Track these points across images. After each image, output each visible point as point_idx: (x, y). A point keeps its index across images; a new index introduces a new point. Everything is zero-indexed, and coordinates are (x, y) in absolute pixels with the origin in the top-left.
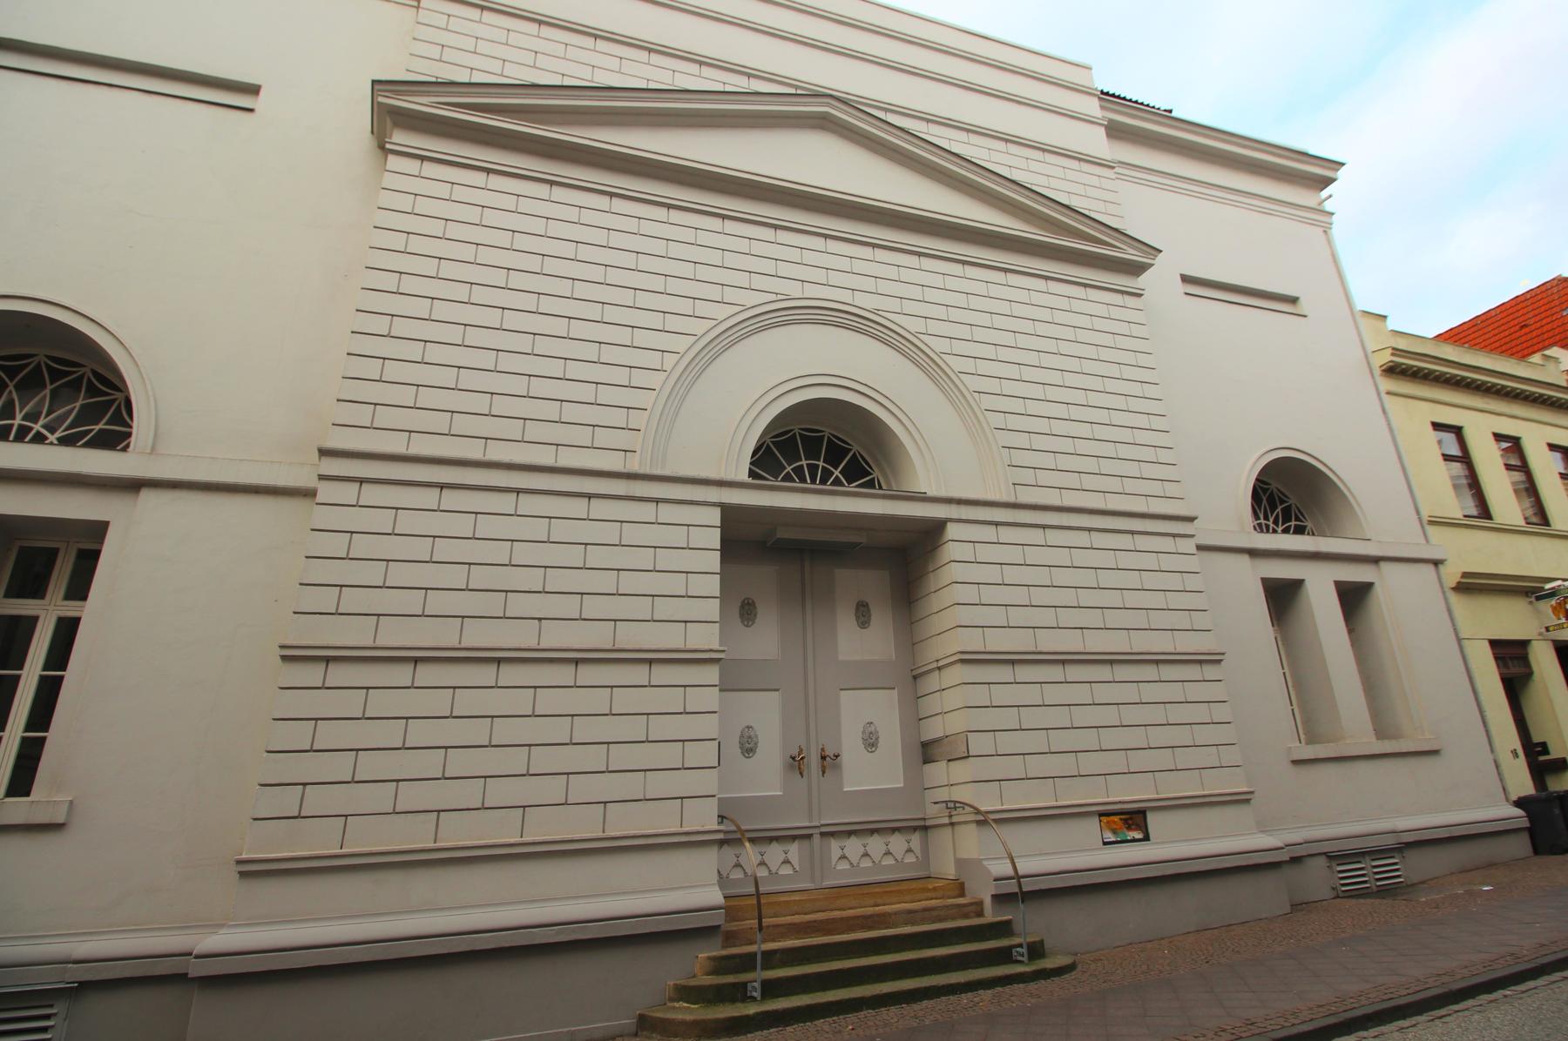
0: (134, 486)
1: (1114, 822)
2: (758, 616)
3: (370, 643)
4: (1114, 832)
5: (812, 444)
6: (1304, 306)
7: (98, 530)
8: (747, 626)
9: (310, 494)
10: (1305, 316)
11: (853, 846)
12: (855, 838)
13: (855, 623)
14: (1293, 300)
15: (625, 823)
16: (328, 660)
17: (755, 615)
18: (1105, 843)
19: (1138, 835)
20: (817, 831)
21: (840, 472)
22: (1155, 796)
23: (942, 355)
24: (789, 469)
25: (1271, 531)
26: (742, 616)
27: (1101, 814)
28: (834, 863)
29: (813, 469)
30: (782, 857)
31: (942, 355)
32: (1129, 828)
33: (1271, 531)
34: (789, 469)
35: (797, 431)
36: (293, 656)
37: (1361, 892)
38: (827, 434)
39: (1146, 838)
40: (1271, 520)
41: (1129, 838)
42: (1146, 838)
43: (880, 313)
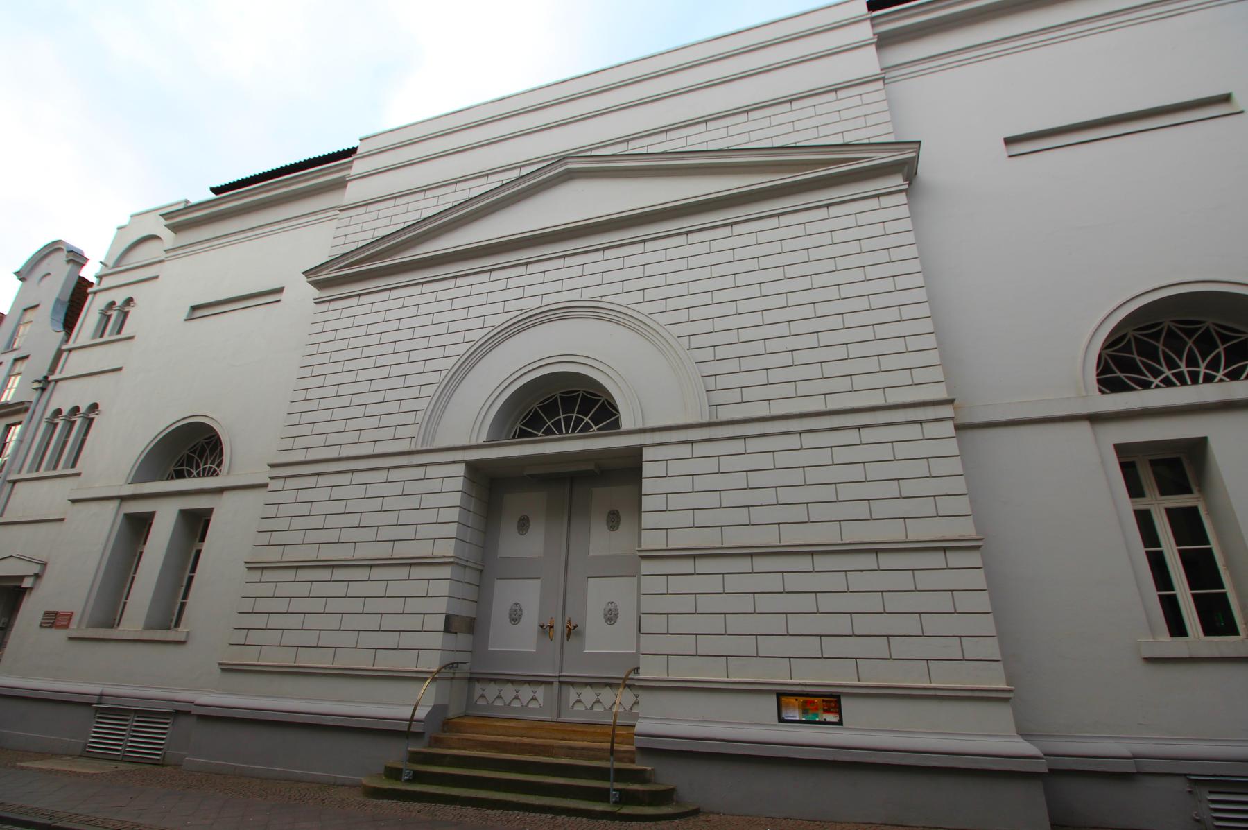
0: (220, 491)
1: (813, 702)
2: (531, 527)
3: (279, 559)
4: (805, 712)
5: (568, 402)
6: (1239, 102)
7: (210, 511)
8: (522, 535)
9: (265, 486)
10: (1241, 112)
11: (588, 695)
12: (628, 690)
13: (606, 527)
14: (1226, 99)
15: (387, 662)
16: (333, 567)
17: (528, 527)
18: (781, 720)
19: (831, 718)
20: (556, 680)
21: (589, 419)
22: (856, 683)
23: (649, 316)
24: (549, 423)
25: (1201, 380)
26: (518, 527)
27: (780, 695)
28: (571, 705)
29: (568, 420)
30: (531, 695)
31: (652, 316)
32: (827, 711)
33: (1201, 380)
34: (549, 423)
35: (558, 395)
36: (252, 567)
37: (101, 756)
38: (581, 393)
39: (840, 723)
40: (1165, 369)
41: (817, 720)
42: (840, 723)
43: (604, 299)
